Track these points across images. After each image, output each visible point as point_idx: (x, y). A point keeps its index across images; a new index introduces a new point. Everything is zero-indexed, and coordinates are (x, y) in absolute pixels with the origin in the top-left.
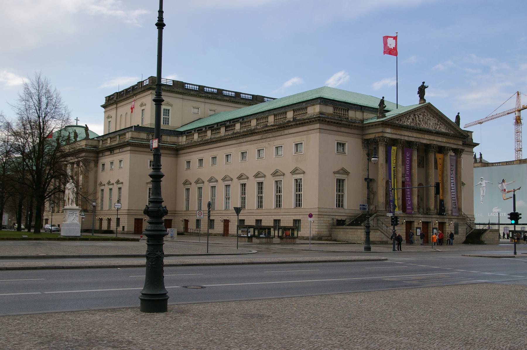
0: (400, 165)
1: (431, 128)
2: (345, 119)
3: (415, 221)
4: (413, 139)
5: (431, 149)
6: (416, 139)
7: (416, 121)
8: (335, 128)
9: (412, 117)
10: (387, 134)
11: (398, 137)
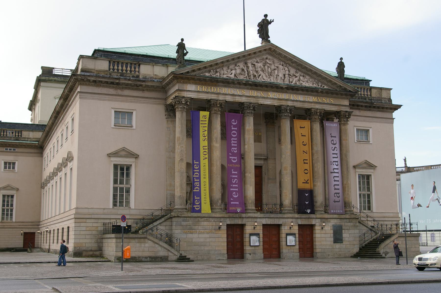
0: (217, 139)
1: (279, 81)
2: (133, 77)
3: (248, 224)
4: (243, 100)
5: (283, 113)
6: (250, 99)
7: (248, 72)
8: (112, 91)
10: (188, 93)
11: (213, 97)
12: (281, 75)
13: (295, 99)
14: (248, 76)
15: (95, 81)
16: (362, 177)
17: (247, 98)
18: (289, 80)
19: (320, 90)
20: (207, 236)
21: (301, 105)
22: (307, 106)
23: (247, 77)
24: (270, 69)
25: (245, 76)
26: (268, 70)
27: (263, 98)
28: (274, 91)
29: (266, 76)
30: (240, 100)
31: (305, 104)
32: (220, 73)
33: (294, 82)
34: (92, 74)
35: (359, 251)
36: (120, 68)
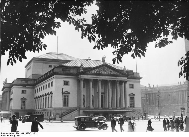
9: (98, 70)
16: (131, 98)
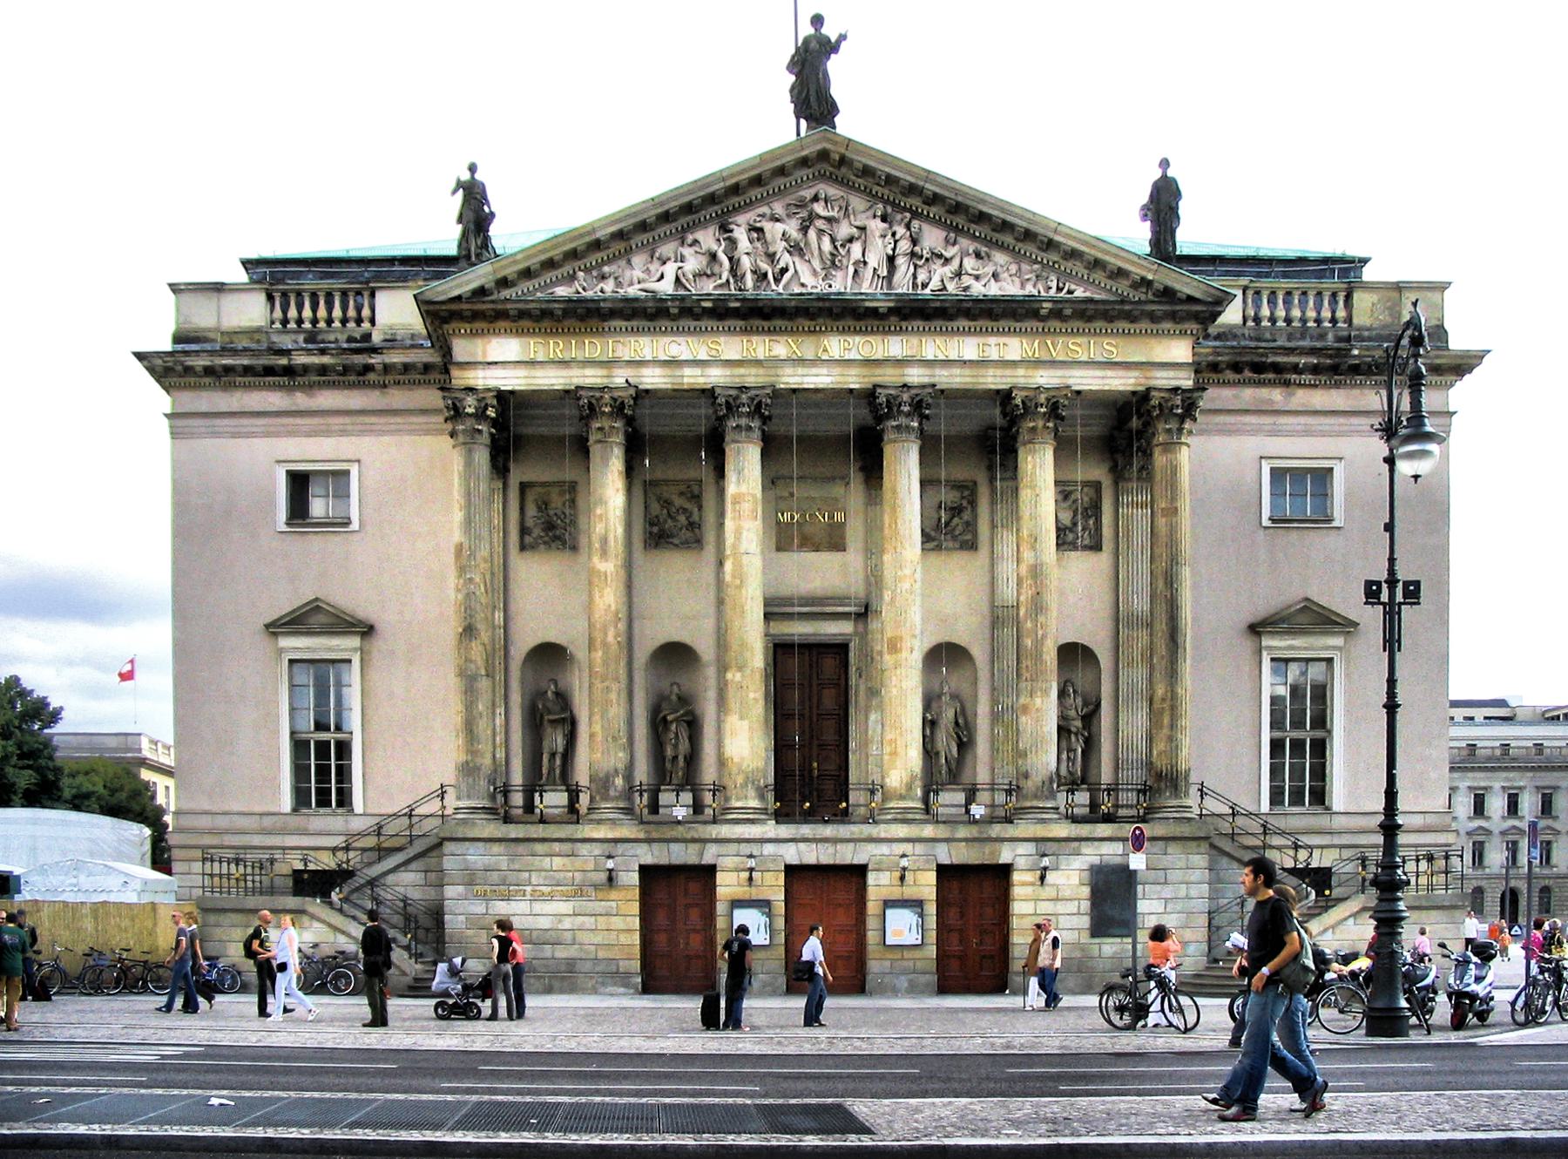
4: (715, 377)
6: (742, 371)
11: (591, 377)
12: (875, 259)
13: (941, 357)
14: (736, 282)
15: (209, 371)
17: (728, 372)
18: (915, 276)
19: (1045, 305)
20: (564, 907)
21: (968, 380)
22: (993, 380)
23: (728, 281)
24: (826, 240)
25: (719, 282)
26: (819, 248)
27: (801, 362)
28: (844, 331)
29: (815, 273)
30: (701, 380)
31: (982, 372)
32: (616, 278)
33: (935, 284)
34: (208, 346)
35: (1208, 969)
36: (307, 313)
